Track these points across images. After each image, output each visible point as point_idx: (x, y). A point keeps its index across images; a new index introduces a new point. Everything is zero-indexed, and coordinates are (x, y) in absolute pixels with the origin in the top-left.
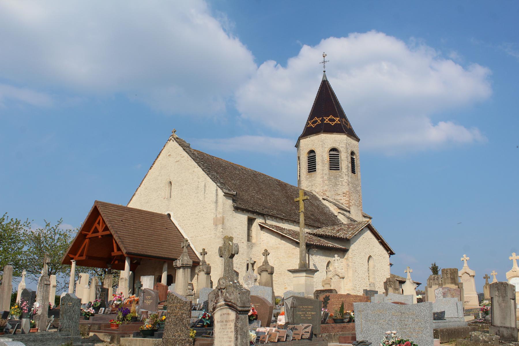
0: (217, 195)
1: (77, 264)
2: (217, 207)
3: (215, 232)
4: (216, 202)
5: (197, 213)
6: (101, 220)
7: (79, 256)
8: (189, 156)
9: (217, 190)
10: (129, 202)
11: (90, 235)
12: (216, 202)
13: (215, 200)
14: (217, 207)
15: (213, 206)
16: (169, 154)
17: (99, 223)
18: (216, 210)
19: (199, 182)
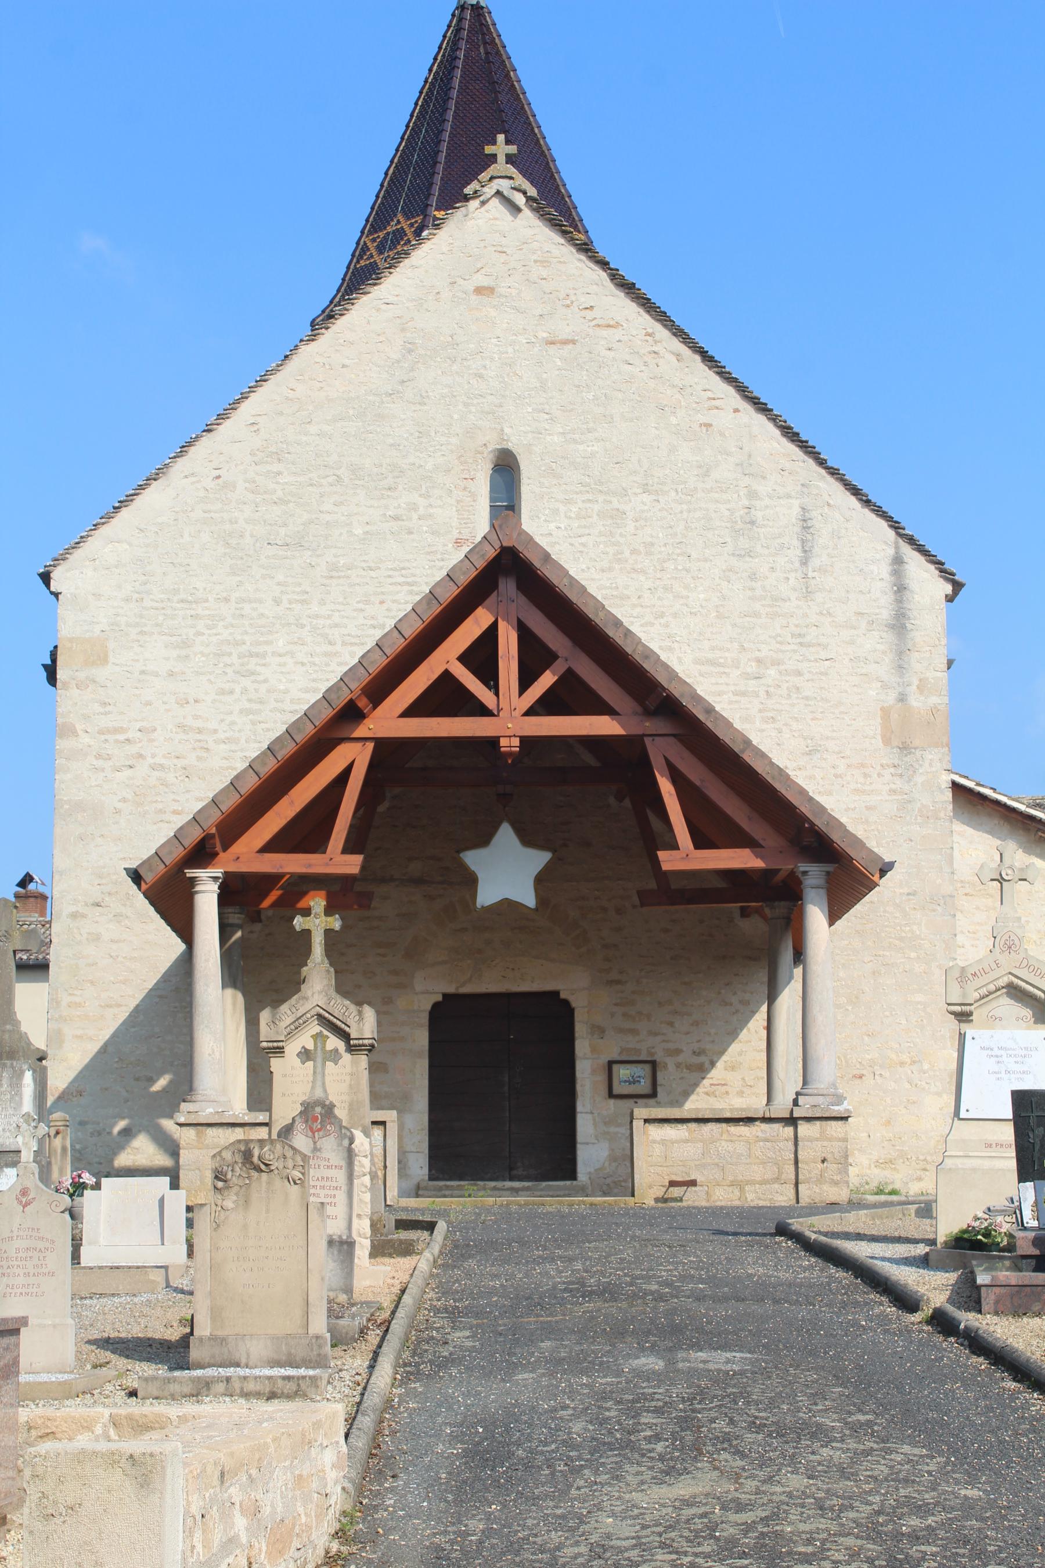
0: (900, 589)
1: (224, 900)
2: (901, 653)
3: (899, 784)
4: (899, 623)
5: (752, 668)
6: (508, 642)
7: (275, 845)
8: (662, 333)
9: (898, 561)
10: (108, 517)
11: (388, 721)
12: (899, 623)
13: (886, 614)
14: (901, 653)
15: (876, 643)
16: (481, 280)
17: (482, 657)
18: (900, 668)
19: (752, 495)
